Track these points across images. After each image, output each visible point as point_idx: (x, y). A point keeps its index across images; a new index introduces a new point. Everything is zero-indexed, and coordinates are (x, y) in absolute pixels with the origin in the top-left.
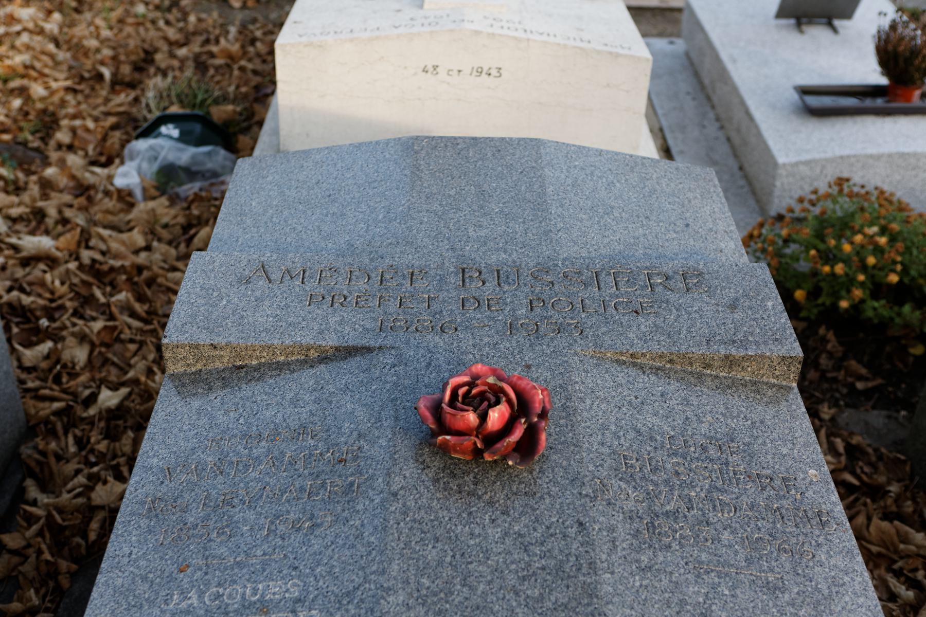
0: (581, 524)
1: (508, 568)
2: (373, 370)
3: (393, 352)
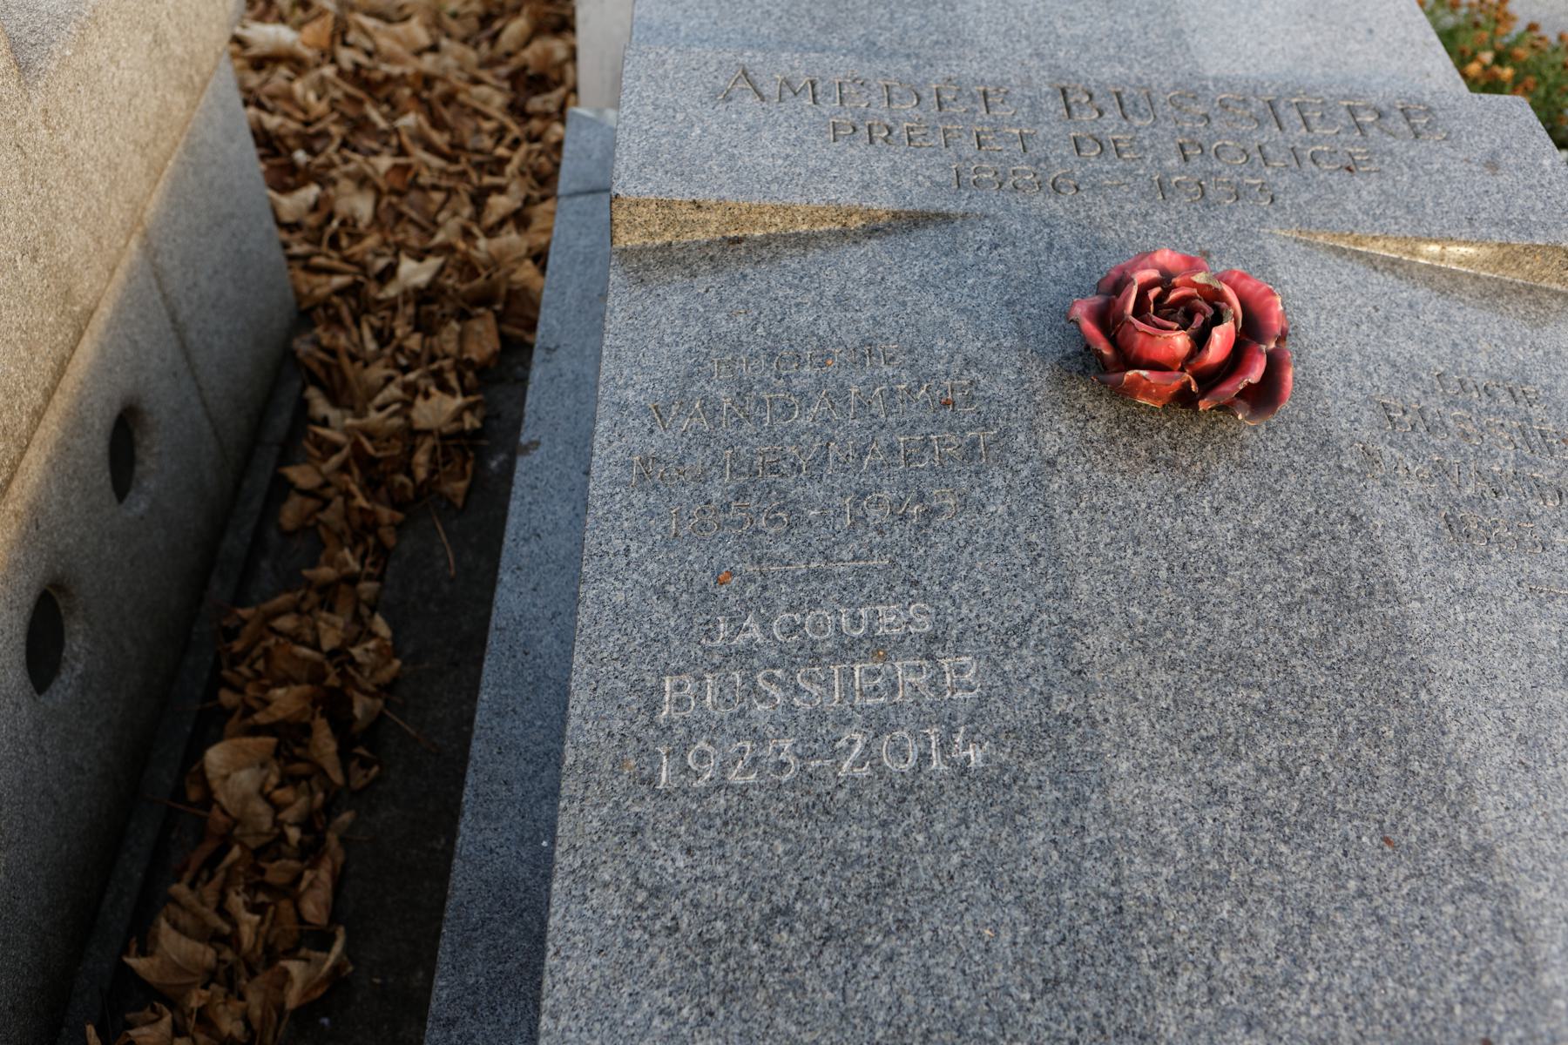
0: (1354, 517)
1: (1259, 589)
2: (961, 252)
3: (987, 223)
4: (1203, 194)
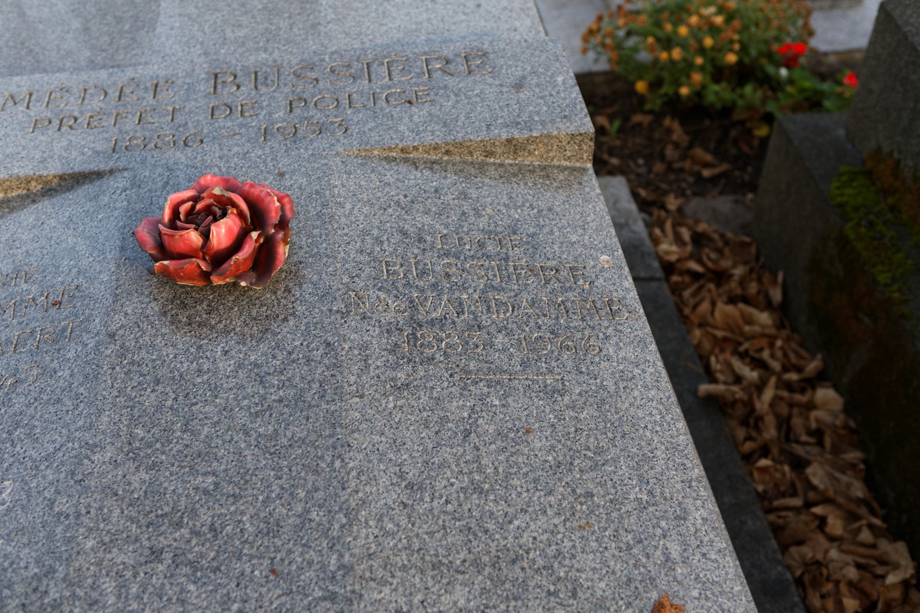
0: (328, 344)
1: (238, 405)
2: (101, 197)
3: (126, 174)
4: (295, 134)
